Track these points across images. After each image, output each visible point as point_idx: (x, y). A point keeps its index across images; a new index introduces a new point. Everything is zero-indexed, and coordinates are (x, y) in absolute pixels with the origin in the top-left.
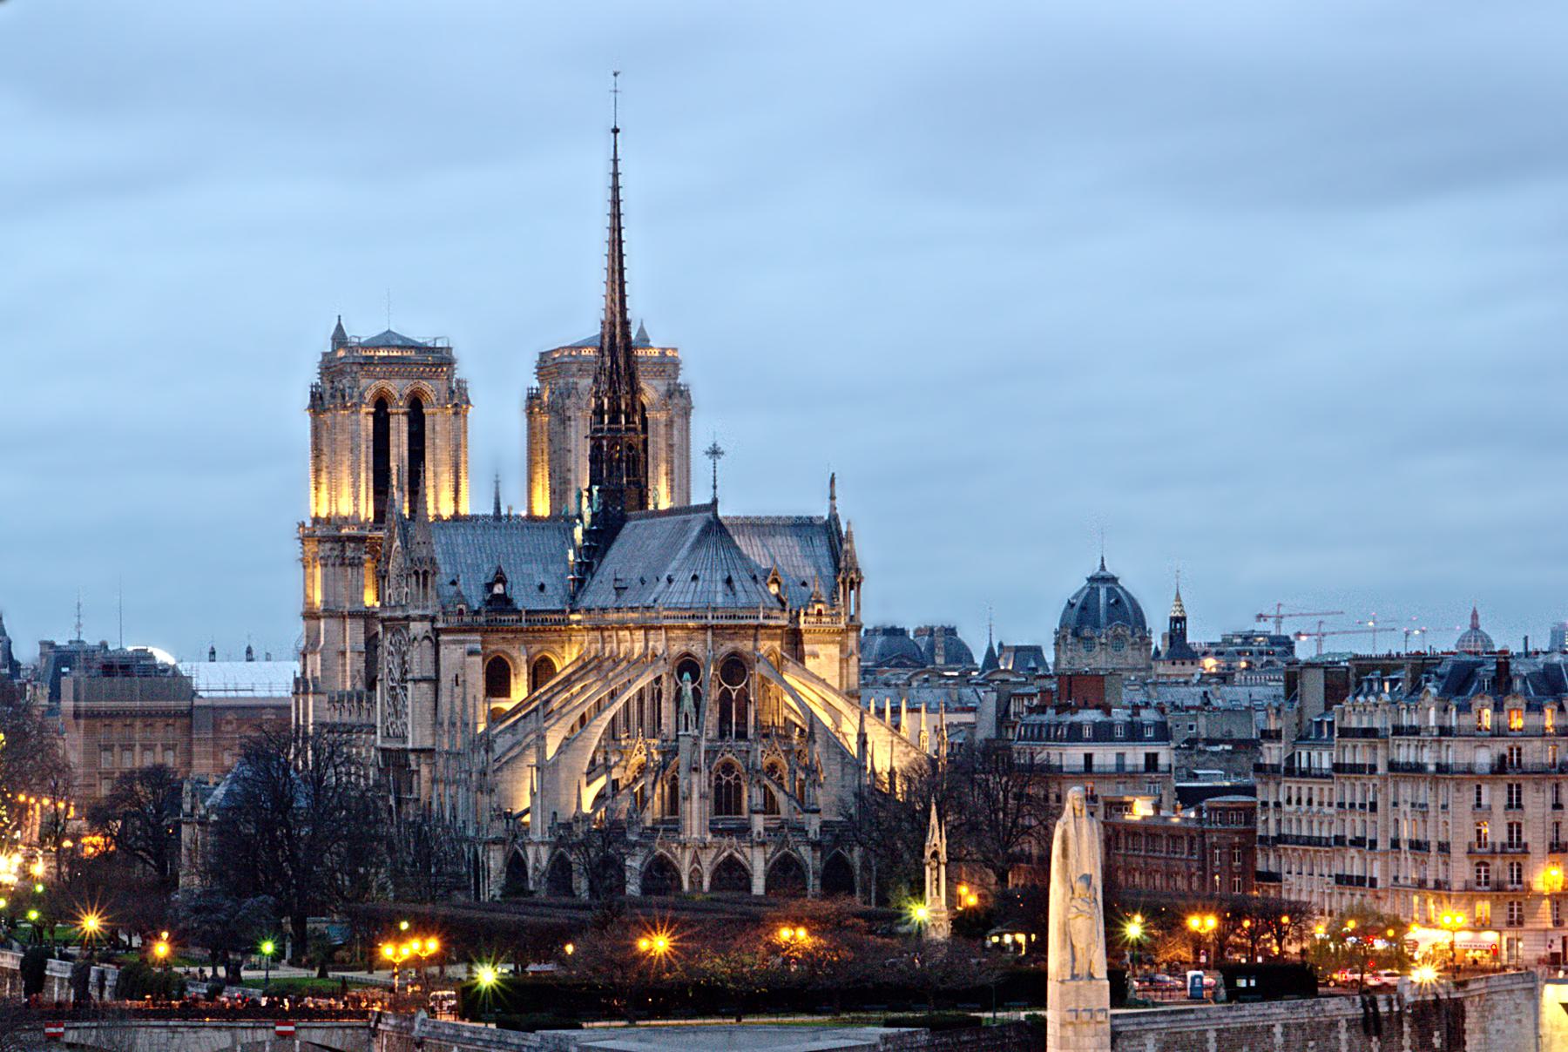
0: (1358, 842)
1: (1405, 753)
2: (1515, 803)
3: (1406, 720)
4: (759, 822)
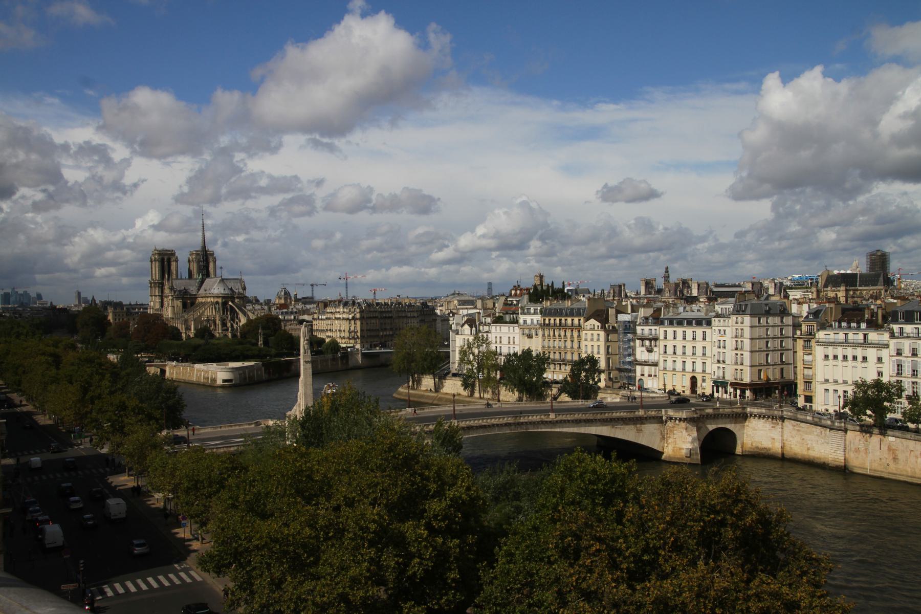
0: (330, 330)
1: (337, 316)
2: (355, 324)
3: (337, 310)
4: (230, 329)
